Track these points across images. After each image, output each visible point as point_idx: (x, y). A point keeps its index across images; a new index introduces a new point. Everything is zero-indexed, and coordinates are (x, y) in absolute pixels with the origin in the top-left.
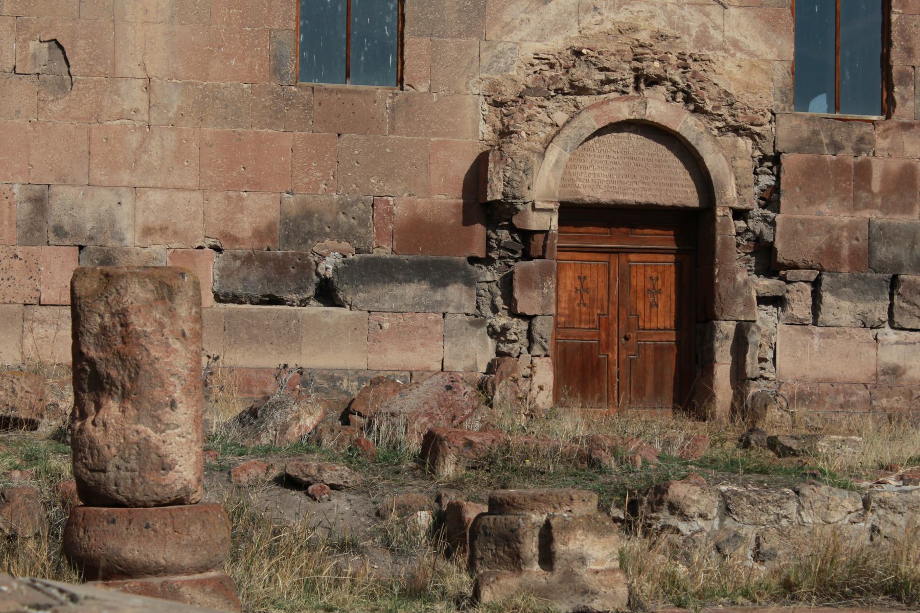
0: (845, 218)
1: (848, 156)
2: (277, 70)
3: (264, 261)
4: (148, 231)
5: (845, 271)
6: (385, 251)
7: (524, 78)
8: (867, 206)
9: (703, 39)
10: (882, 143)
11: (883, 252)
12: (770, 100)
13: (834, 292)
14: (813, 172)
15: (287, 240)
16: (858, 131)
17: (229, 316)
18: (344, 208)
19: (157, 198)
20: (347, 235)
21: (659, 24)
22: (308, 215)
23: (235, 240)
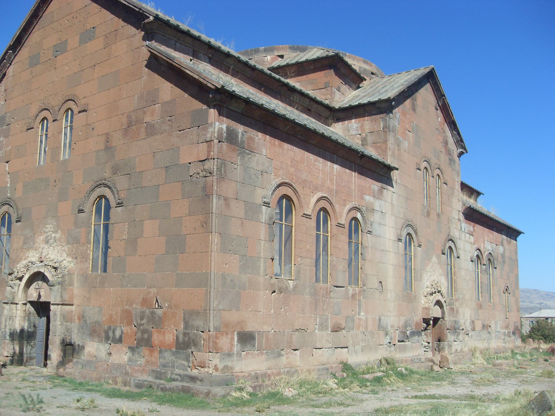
17: (400, 345)
19: (392, 318)
20: (411, 326)
23: (399, 327)
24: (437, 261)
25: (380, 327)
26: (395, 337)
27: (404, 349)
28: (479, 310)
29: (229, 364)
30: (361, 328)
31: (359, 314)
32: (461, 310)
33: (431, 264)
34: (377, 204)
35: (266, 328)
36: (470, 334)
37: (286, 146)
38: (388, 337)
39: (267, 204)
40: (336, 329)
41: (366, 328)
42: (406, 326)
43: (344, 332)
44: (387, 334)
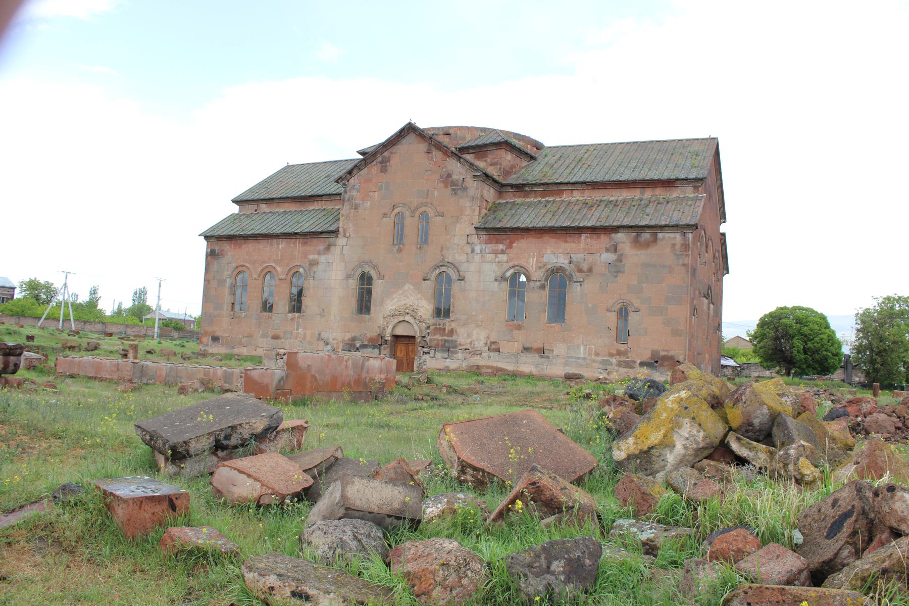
0: (440, 338)
1: (442, 326)
2: (352, 313)
3: (349, 344)
4: (333, 339)
5: (440, 348)
6: (366, 343)
7: (388, 313)
8: (445, 336)
9: (418, 306)
10: (447, 324)
11: (447, 344)
12: (429, 317)
13: (438, 352)
14: (436, 329)
15: (352, 341)
16: (444, 322)
18: (360, 335)
19: (335, 334)
21: (411, 303)
22: (355, 337)
23: (344, 341)
24: (412, 287)
25: (319, 338)
26: (338, 348)
28: (516, 332)
29: (207, 349)
30: (298, 339)
31: (297, 329)
34: (322, 259)
35: (226, 335)
36: (484, 354)
38: (328, 346)
39: (230, 277)
40: (276, 337)
41: (304, 338)
42: (354, 339)
43: (283, 340)
44: (327, 344)
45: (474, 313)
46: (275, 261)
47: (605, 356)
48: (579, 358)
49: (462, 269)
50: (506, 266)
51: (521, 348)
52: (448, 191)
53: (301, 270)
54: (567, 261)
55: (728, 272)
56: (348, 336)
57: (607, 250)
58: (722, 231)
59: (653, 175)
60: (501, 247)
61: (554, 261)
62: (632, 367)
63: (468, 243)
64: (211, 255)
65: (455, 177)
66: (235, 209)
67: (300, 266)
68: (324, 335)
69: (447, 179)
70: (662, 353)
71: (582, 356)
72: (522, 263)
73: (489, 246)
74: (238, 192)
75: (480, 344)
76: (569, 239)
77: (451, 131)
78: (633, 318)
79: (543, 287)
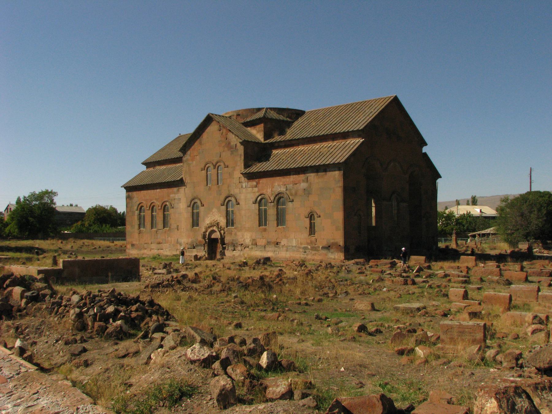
24: (216, 210)
25: (178, 242)
27: (192, 252)
31: (168, 238)
32: (239, 234)
33: (212, 213)
34: (177, 196)
36: (250, 247)
37: (142, 192)
39: (137, 210)
40: (159, 243)
41: (171, 242)
45: (244, 223)
46: (156, 199)
47: (305, 245)
48: (293, 246)
49: (238, 198)
50: (257, 194)
51: (266, 242)
52: (229, 153)
53: (167, 203)
54: (285, 190)
55: (439, 176)
56: (190, 240)
57: (303, 181)
58: (423, 151)
59: (338, 130)
60: (254, 183)
61: (279, 190)
62: (318, 251)
63: (240, 182)
64: (128, 198)
65: (232, 144)
66: (144, 168)
67: (167, 201)
68: (180, 240)
69: (228, 145)
70: (332, 241)
71: (294, 245)
72: (264, 192)
73: (249, 183)
74: (145, 158)
75: (248, 241)
76: (285, 177)
77: (240, 113)
78: (317, 221)
79: (274, 206)
